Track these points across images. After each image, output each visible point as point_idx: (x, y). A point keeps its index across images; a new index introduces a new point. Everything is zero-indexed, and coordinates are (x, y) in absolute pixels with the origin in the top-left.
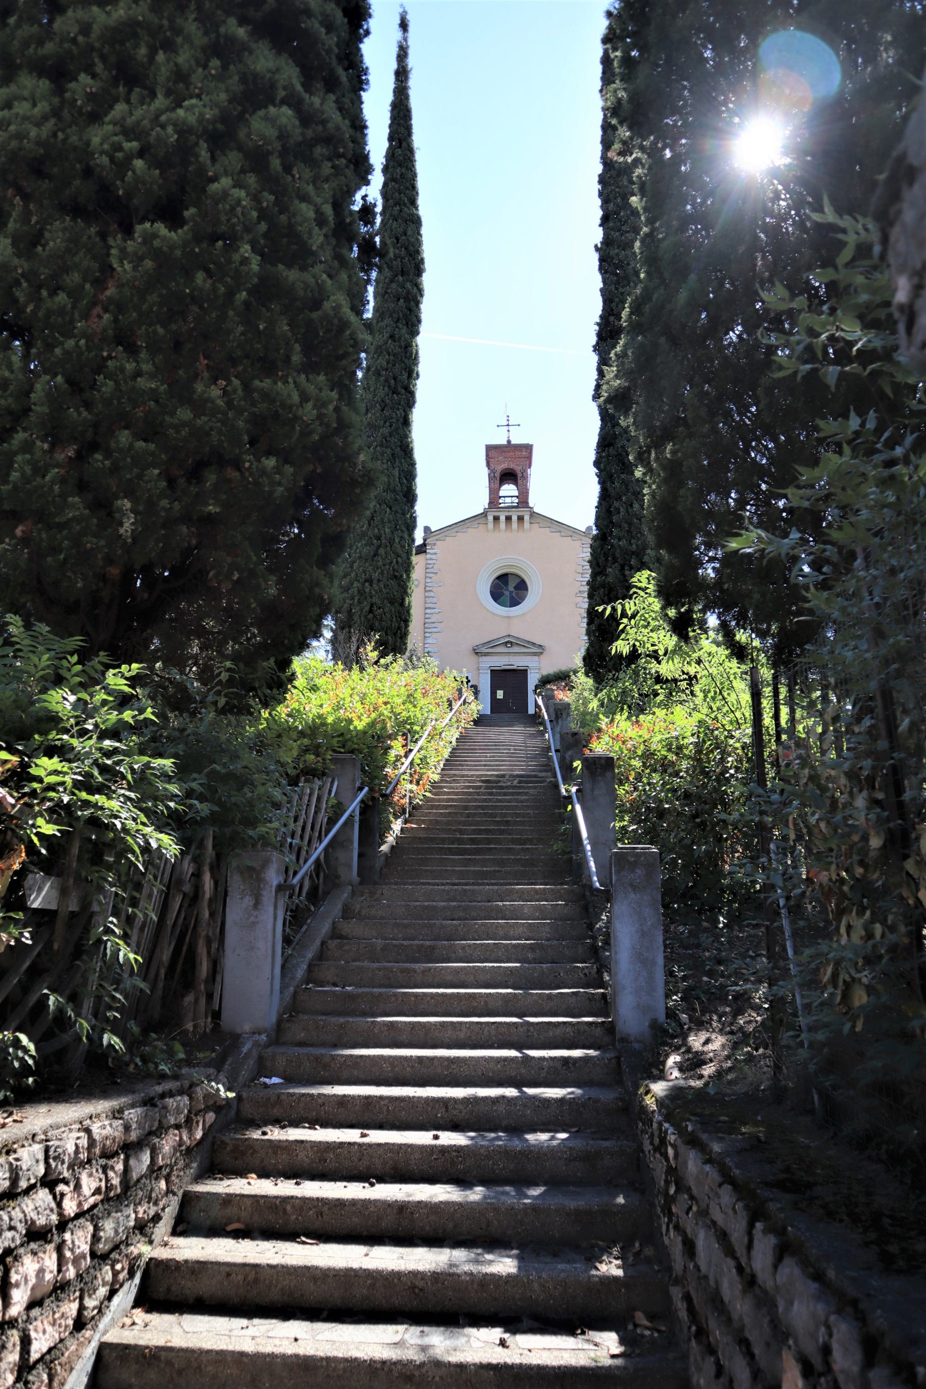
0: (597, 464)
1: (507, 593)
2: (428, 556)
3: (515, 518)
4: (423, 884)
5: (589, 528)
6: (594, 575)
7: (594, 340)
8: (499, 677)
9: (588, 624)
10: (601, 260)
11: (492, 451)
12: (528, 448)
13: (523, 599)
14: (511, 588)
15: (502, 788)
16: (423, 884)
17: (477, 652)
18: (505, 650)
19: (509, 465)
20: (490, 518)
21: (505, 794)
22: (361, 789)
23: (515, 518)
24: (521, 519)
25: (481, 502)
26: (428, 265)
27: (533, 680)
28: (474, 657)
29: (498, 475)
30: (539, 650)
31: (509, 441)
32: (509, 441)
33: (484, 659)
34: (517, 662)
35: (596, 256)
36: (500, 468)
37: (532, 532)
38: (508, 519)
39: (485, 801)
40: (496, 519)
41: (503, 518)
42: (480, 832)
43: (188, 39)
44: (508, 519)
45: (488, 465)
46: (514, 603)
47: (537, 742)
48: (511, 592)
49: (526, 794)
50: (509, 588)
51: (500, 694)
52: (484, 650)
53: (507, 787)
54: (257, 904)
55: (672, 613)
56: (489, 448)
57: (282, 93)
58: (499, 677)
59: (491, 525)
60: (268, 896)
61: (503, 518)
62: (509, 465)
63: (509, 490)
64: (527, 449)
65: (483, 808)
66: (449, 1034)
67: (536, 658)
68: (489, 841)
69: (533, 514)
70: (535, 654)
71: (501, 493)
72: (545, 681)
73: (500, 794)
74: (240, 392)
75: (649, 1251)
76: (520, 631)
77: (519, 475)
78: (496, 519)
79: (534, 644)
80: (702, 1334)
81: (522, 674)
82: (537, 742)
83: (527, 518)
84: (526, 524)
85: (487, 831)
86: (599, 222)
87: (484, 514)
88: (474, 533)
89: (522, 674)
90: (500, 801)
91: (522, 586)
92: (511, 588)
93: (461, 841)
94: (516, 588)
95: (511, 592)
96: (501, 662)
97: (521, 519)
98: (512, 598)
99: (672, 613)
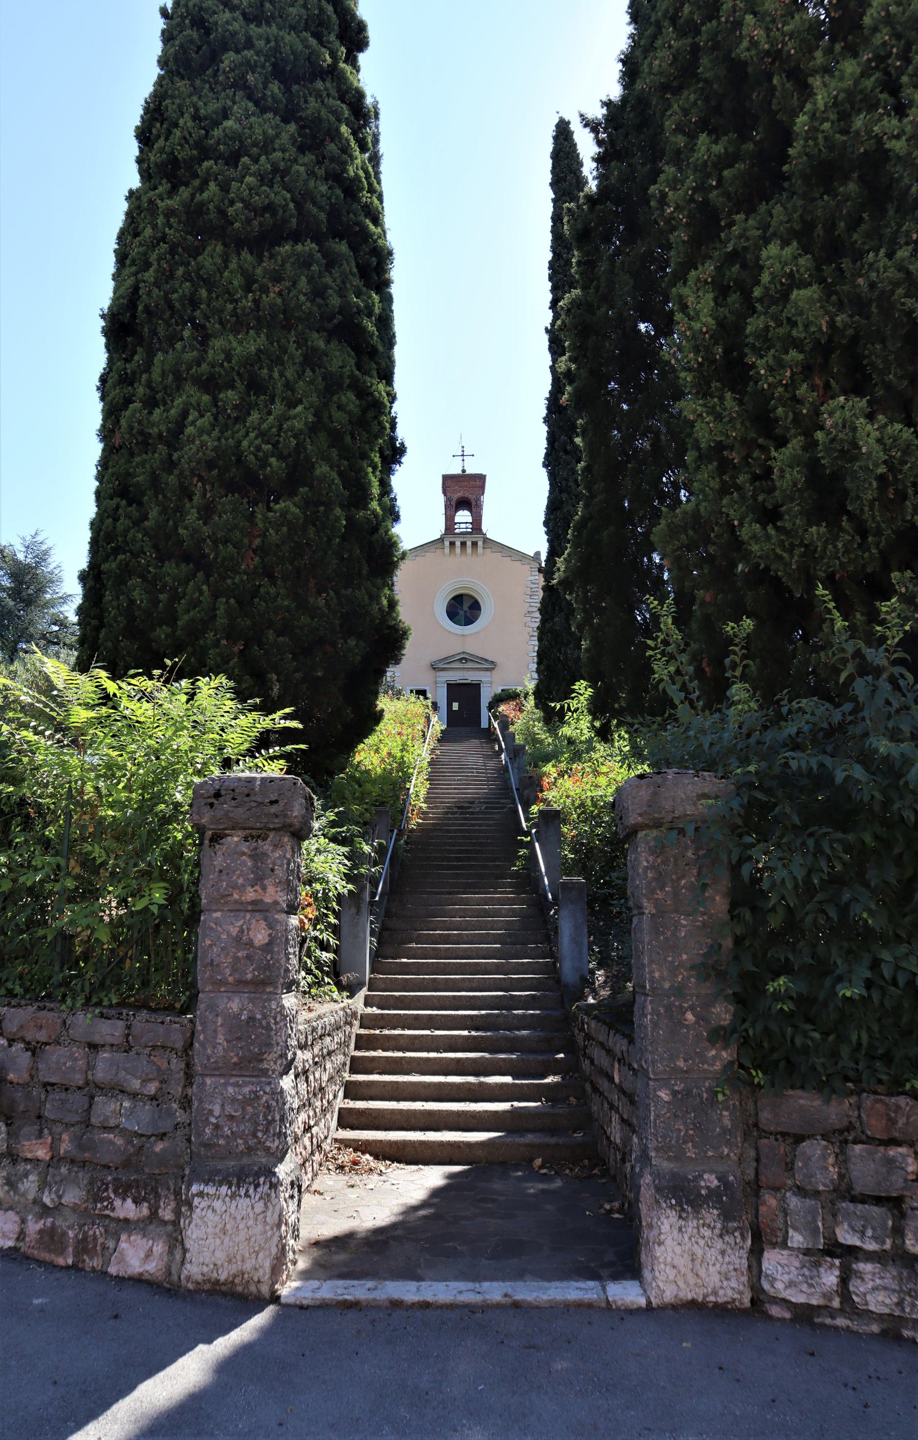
0: (546, 524)
1: (461, 613)
3: (469, 544)
4: (429, 893)
5: (538, 554)
6: (543, 622)
7: (544, 412)
8: (456, 691)
9: (538, 664)
10: (551, 341)
11: (447, 479)
14: (466, 608)
15: (473, 813)
16: (429, 893)
17: (434, 667)
18: (461, 666)
19: (463, 492)
20: (447, 543)
21: (476, 819)
22: (392, 831)
23: (469, 544)
24: (475, 544)
25: (437, 529)
26: (398, 338)
27: (486, 698)
28: (432, 672)
29: (453, 503)
30: (490, 666)
31: (464, 471)
32: (464, 471)
33: (441, 673)
34: (471, 677)
35: (546, 337)
36: (455, 497)
37: (487, 557)
38: (463, 544)
39: (462, 825)
40: (452, 544)
41: (458, 544)
42: (461, 852)
43: (291, 357)
44: (463, 544)
45: (445, 492)
46: (469, 621)
47: (492, 764)
49: (493, 819)
50: (464, 609)
51: (455, 706)
52: (441, 666)
53: (478, 813)
54: (358, 912)
55: (597, 724)
56: (447, 479)
57: (347, 381)
58: (456, 691)
59: (447, 550)
60: (365, 908)
61: (458, 544)
63: (463, 517)
64: (479, 481)
65: (461, 831)
66: (467, 984)
67: (488, 673)
68: (469, 859)
69: (486, 540)
70: (487, 670)
71: (457, 520)
72: (499, 700)
73: (472, 819)
74: (335, 600)
75: (576, 1075)
76: (474, 648)
77: (474, 503)
78: (452, 544)
79: (486, 660)
80: (595, 1089)
81: (475, 688)
82: (492, 764)
83: (480, 544)
84: (480, 550)
85: (467, 851)
86: (549, 305)
87: (441, 540)
88: (431, 556)
89: (475, 688)
90: (473, 825)
91: (476, 606)
92: (466, 608)
93: (448, 859)
94: (471, 608)
96: (456, 677)
97: (475, 544)
98: (466, 617)
99: (597, 724)
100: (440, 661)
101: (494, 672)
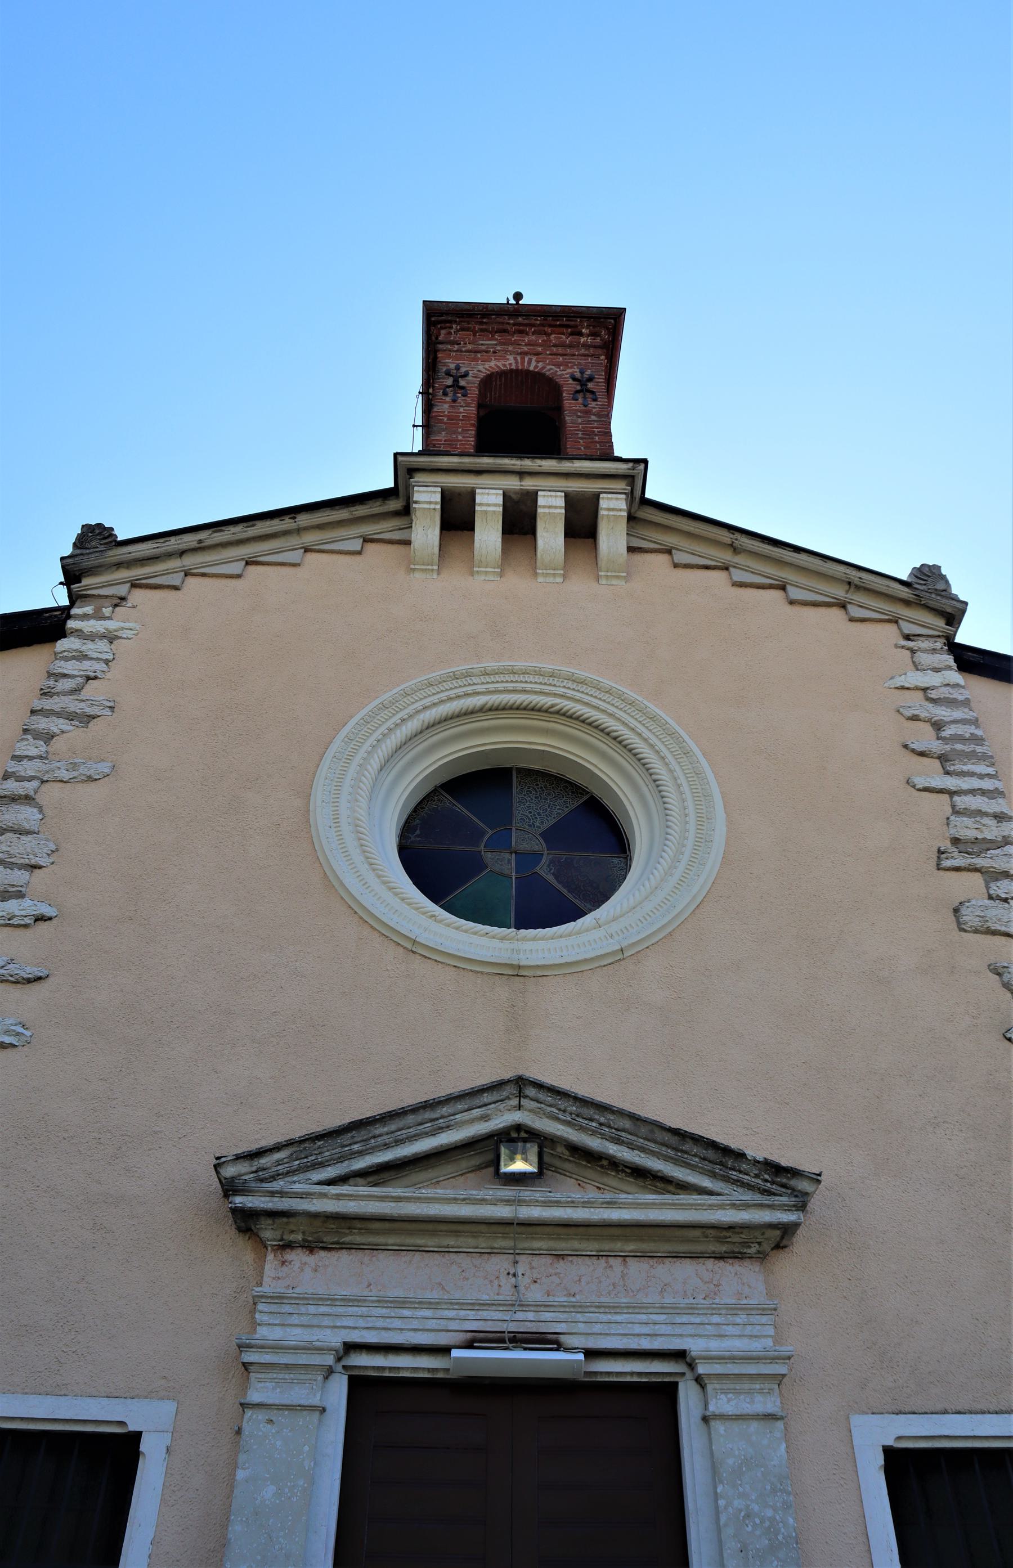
1: (501, 863)
2: (62, 645)
12: (604, 326)
13: (600, 896)
17: (256, 1210)
19: (521, 394)
20: (427, 497)
24: (581, 526)
28: (227, 1258)
29: (471, 383)
36: (480, 368)
40: (457, 518)
46: (544, 908)
48: (527, 859)
50: (513, 833)
52: (312, 1195)
59: (426, 532)
62: (521, 394)
67: (739, 1280)
69: (645, 513)
70: (732, 1244)
77: (569, 387)
79: (723, 1158)
83: (613, 505)
84: (612, 537)
87: (391, 503)
95: (527, 859)
97: (581, 526)
100: (311, 1147)
101: (787, 1267)
